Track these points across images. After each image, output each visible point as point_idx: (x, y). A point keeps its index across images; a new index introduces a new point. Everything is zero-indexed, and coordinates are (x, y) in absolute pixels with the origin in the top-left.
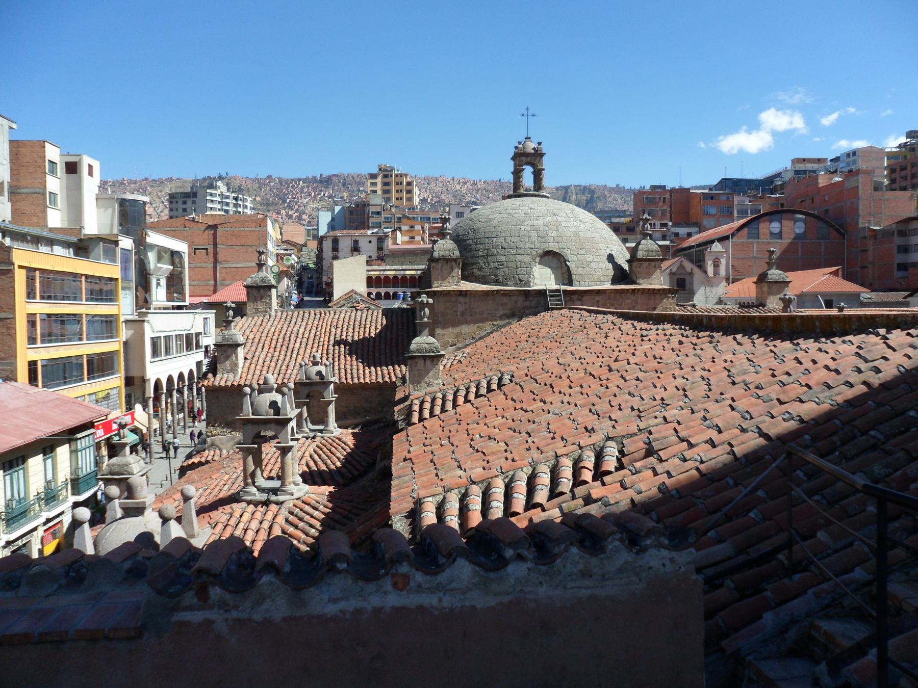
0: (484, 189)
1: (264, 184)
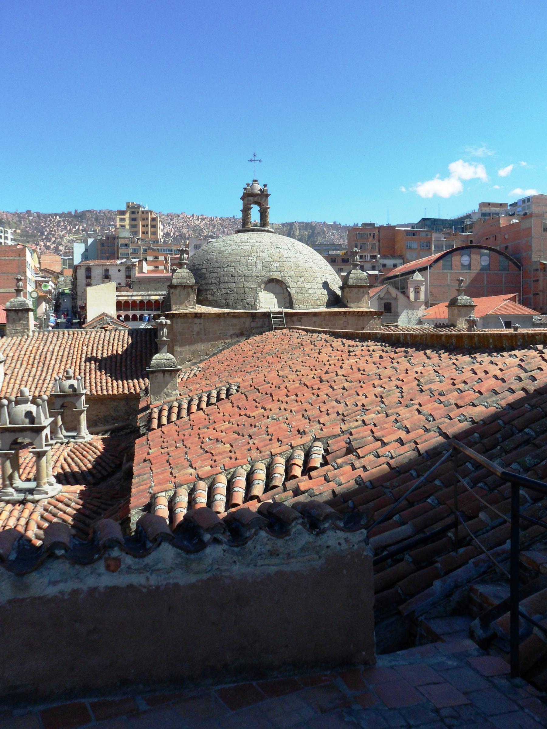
0: (220, 224)
1: (24, 218)
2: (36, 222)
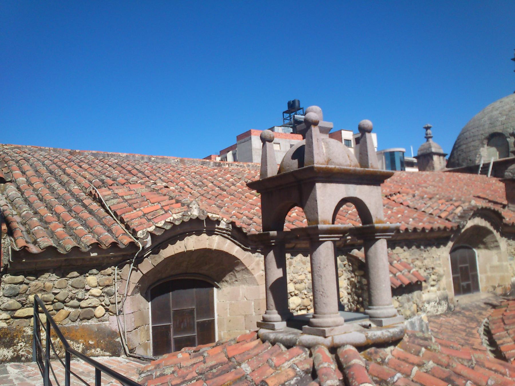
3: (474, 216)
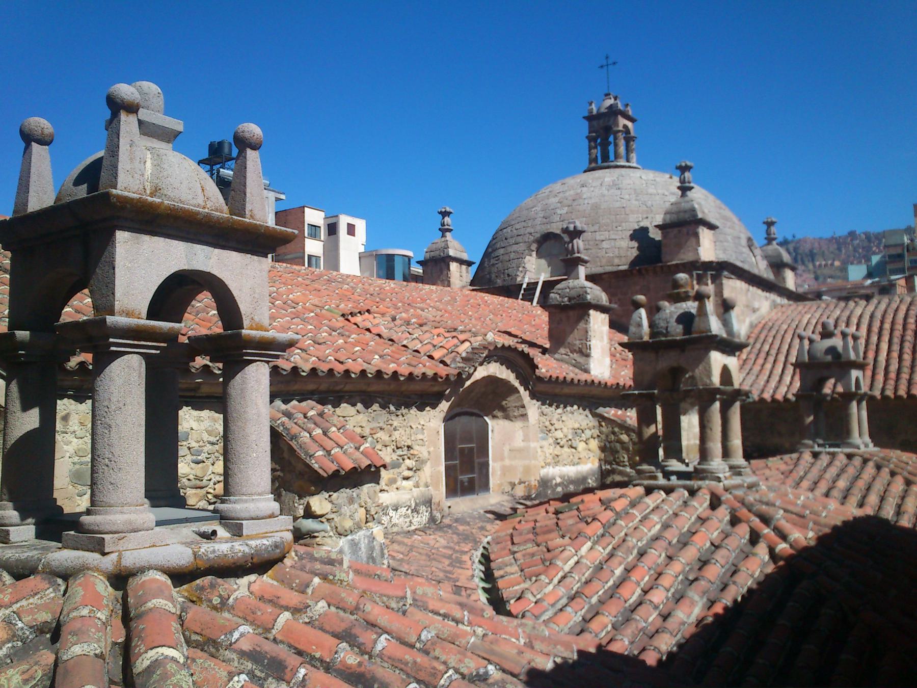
2: (863, 248)
3: (488, 359)
